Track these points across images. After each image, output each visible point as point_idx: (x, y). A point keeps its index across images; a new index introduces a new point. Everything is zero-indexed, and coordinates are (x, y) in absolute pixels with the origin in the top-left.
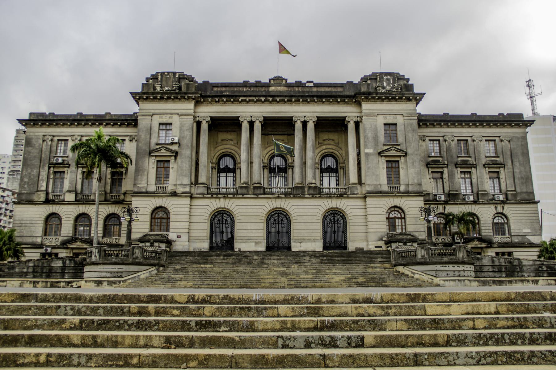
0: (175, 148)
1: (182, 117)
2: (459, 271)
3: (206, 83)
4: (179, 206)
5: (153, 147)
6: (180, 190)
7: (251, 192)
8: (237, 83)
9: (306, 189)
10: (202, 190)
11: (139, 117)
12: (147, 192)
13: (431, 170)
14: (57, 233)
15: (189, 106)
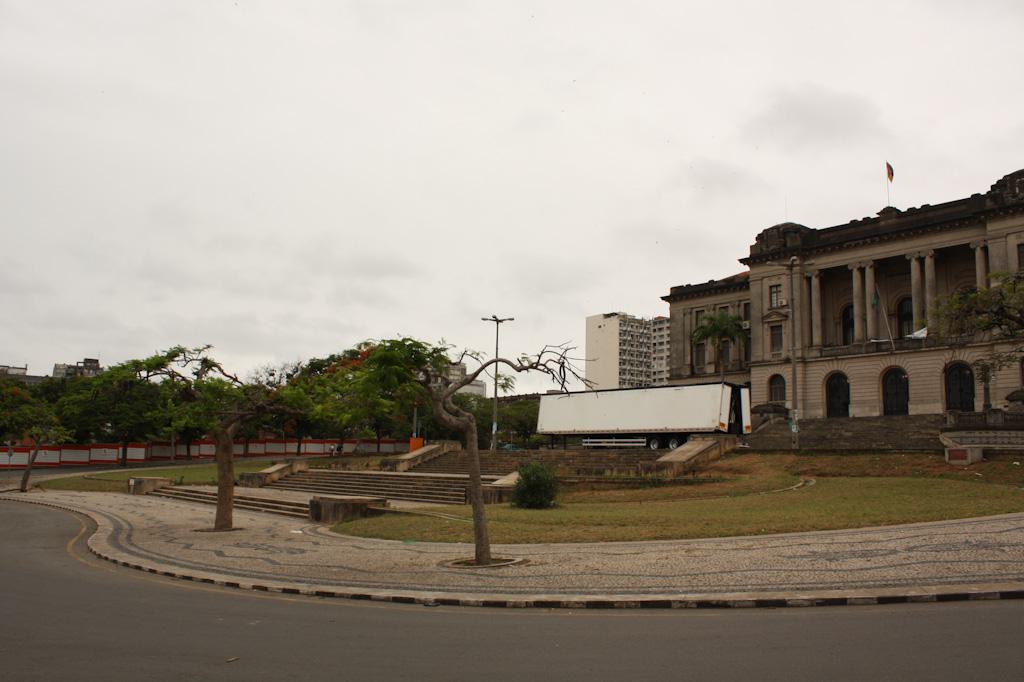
2: (988, 438)
7: (863, 349)
10: (815, 353)
12: (763, 361)
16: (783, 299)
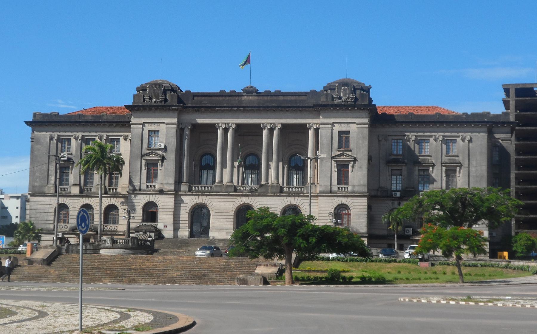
1: (168, 126)
3: (188, 93)
4: (165, 201)
5: (145, 151)
6: (166, 188)
7: (224, 190)
8: (214, 93)
9: (270, 188)
11: (132, 126)
13: (390, 168)
14: (66, 220)
16: (160, 142)
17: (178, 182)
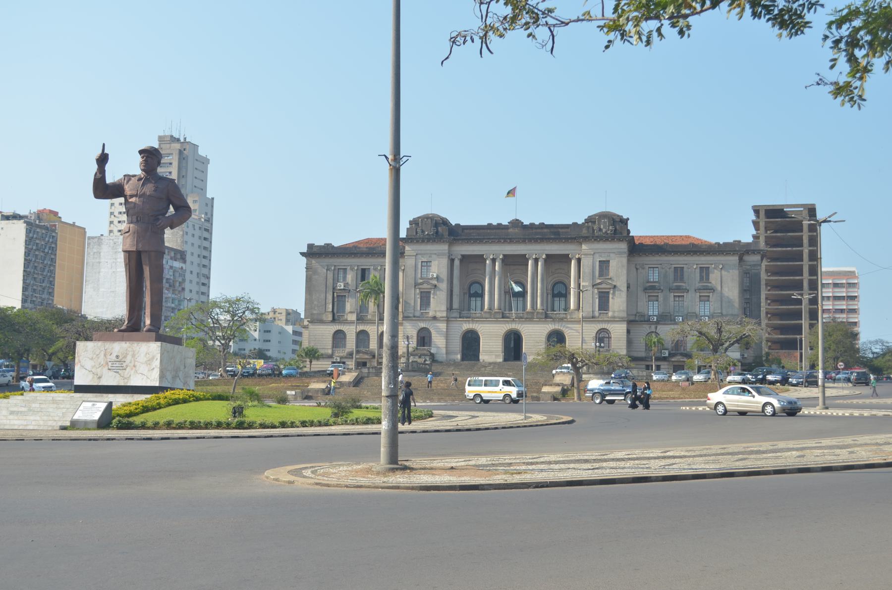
0: (435, 282)
3: (458, 225)
6: (439, 315)
10: (456, 314)
15: (444, 247)
17: (450, 308)
